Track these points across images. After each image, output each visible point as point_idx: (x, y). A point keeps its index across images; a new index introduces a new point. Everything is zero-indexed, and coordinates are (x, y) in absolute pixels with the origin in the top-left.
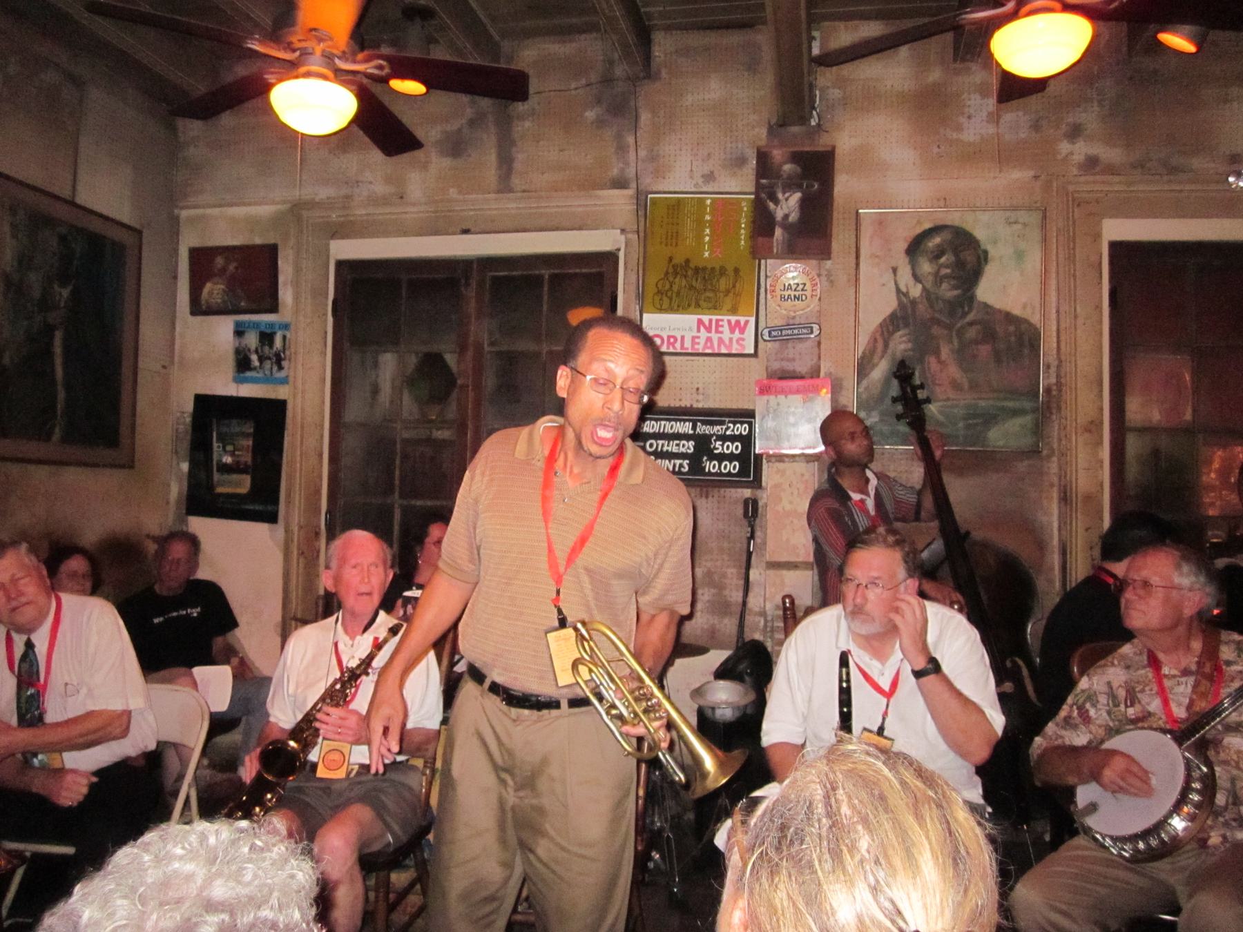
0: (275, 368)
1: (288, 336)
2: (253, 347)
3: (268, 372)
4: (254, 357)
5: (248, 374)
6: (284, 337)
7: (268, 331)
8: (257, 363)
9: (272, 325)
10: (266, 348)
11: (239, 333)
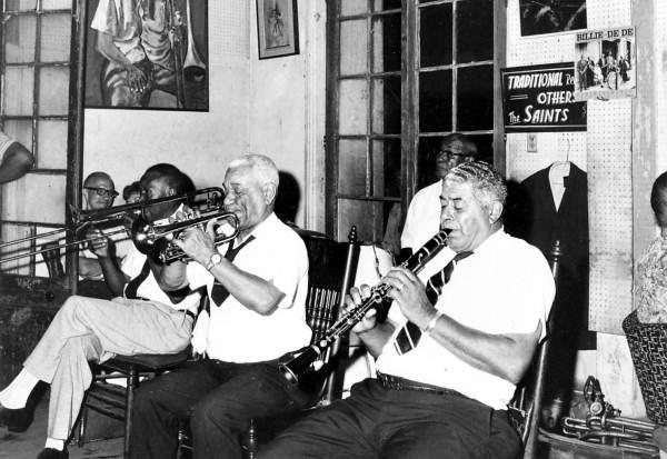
0: (620, 79)
1: (633, 41)
2: (596, 62)
3: (613, 86)
4: (597, 71)
5: (591, 89)
6: (629, 44)
7: (612, 40)
8: (601, 77)
9: (615, 33)
10: (610, 58)
11: (582, 46)
